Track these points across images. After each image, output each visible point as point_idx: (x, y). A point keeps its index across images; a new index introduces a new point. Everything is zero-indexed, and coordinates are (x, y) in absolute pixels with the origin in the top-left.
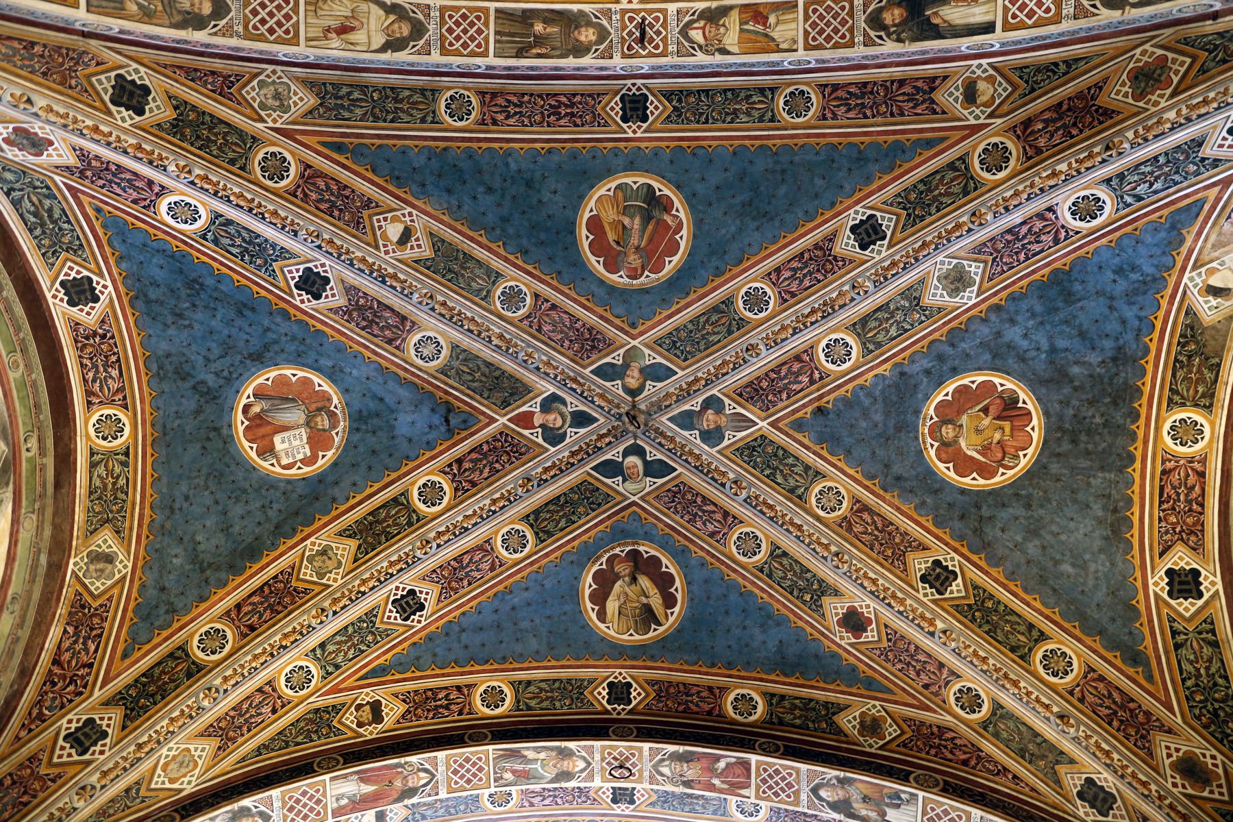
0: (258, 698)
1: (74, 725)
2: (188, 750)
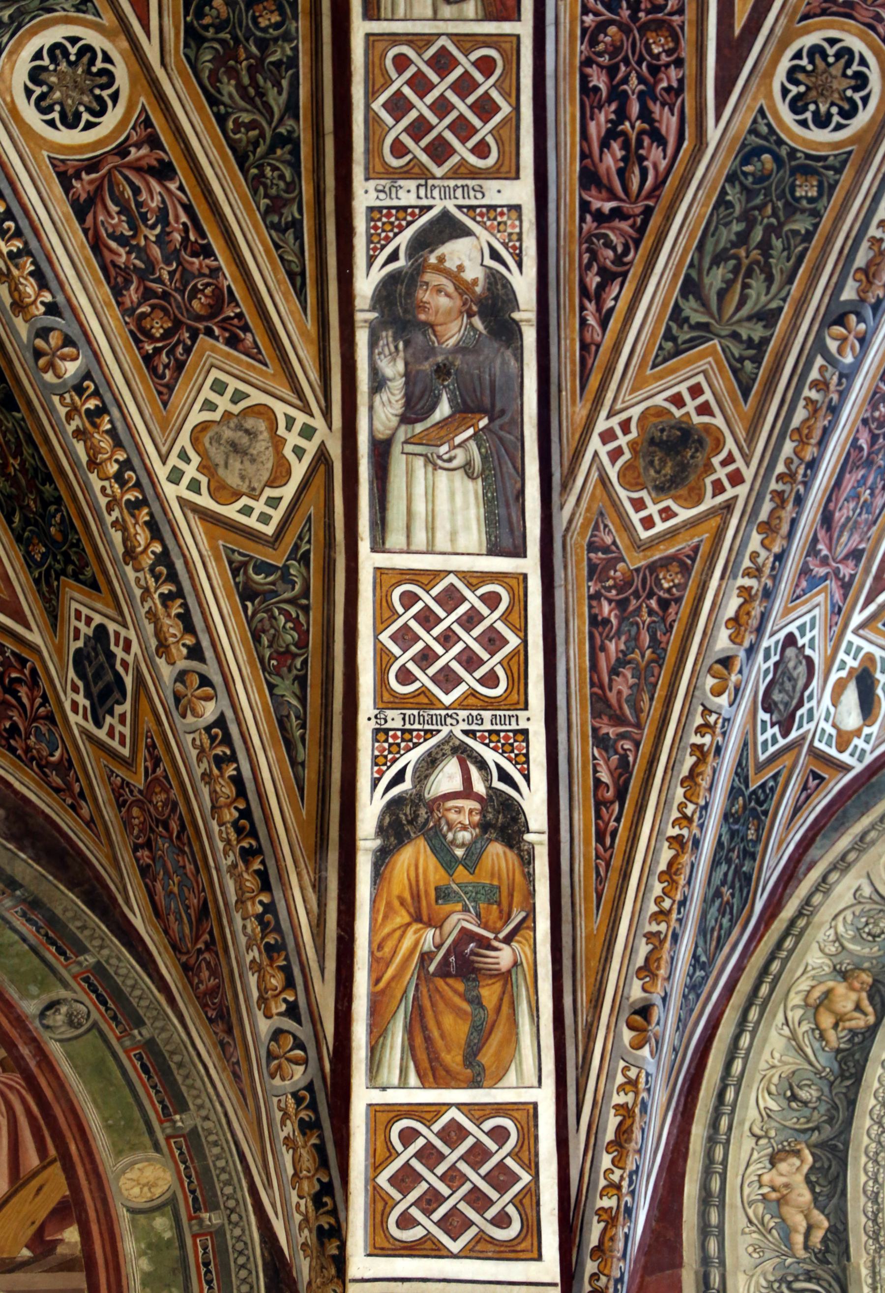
0: (112, 219)
1: (82, 701)
2: (203, 427)
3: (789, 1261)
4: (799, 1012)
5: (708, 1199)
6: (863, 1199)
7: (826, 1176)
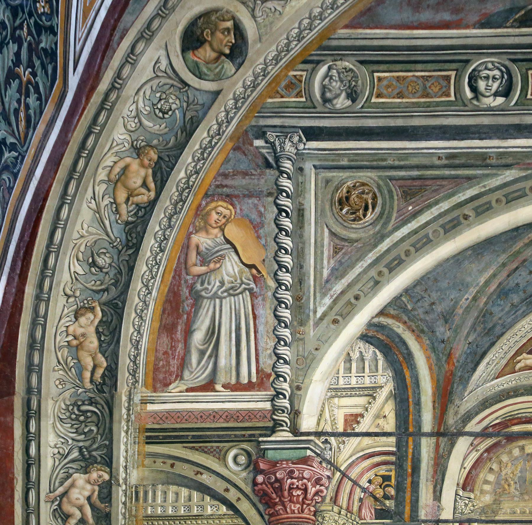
3: (81, 390)
4: (104, 186)
5: (35, 345)
6: (129, 346)
7: (108, 328)
